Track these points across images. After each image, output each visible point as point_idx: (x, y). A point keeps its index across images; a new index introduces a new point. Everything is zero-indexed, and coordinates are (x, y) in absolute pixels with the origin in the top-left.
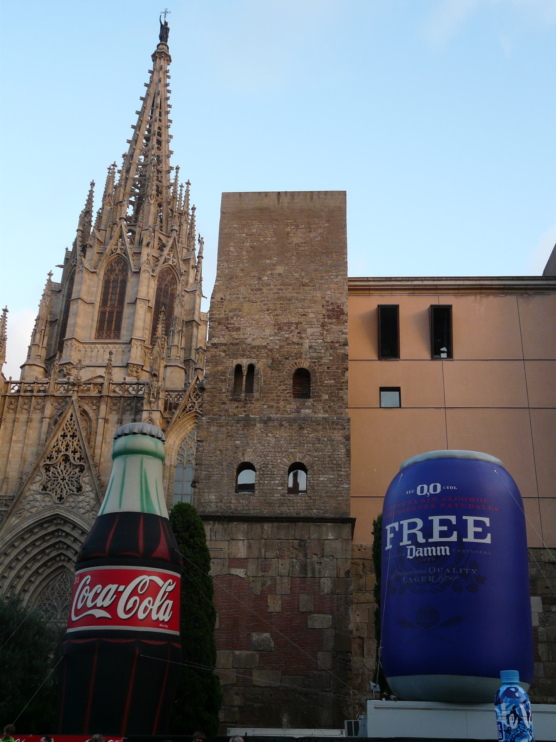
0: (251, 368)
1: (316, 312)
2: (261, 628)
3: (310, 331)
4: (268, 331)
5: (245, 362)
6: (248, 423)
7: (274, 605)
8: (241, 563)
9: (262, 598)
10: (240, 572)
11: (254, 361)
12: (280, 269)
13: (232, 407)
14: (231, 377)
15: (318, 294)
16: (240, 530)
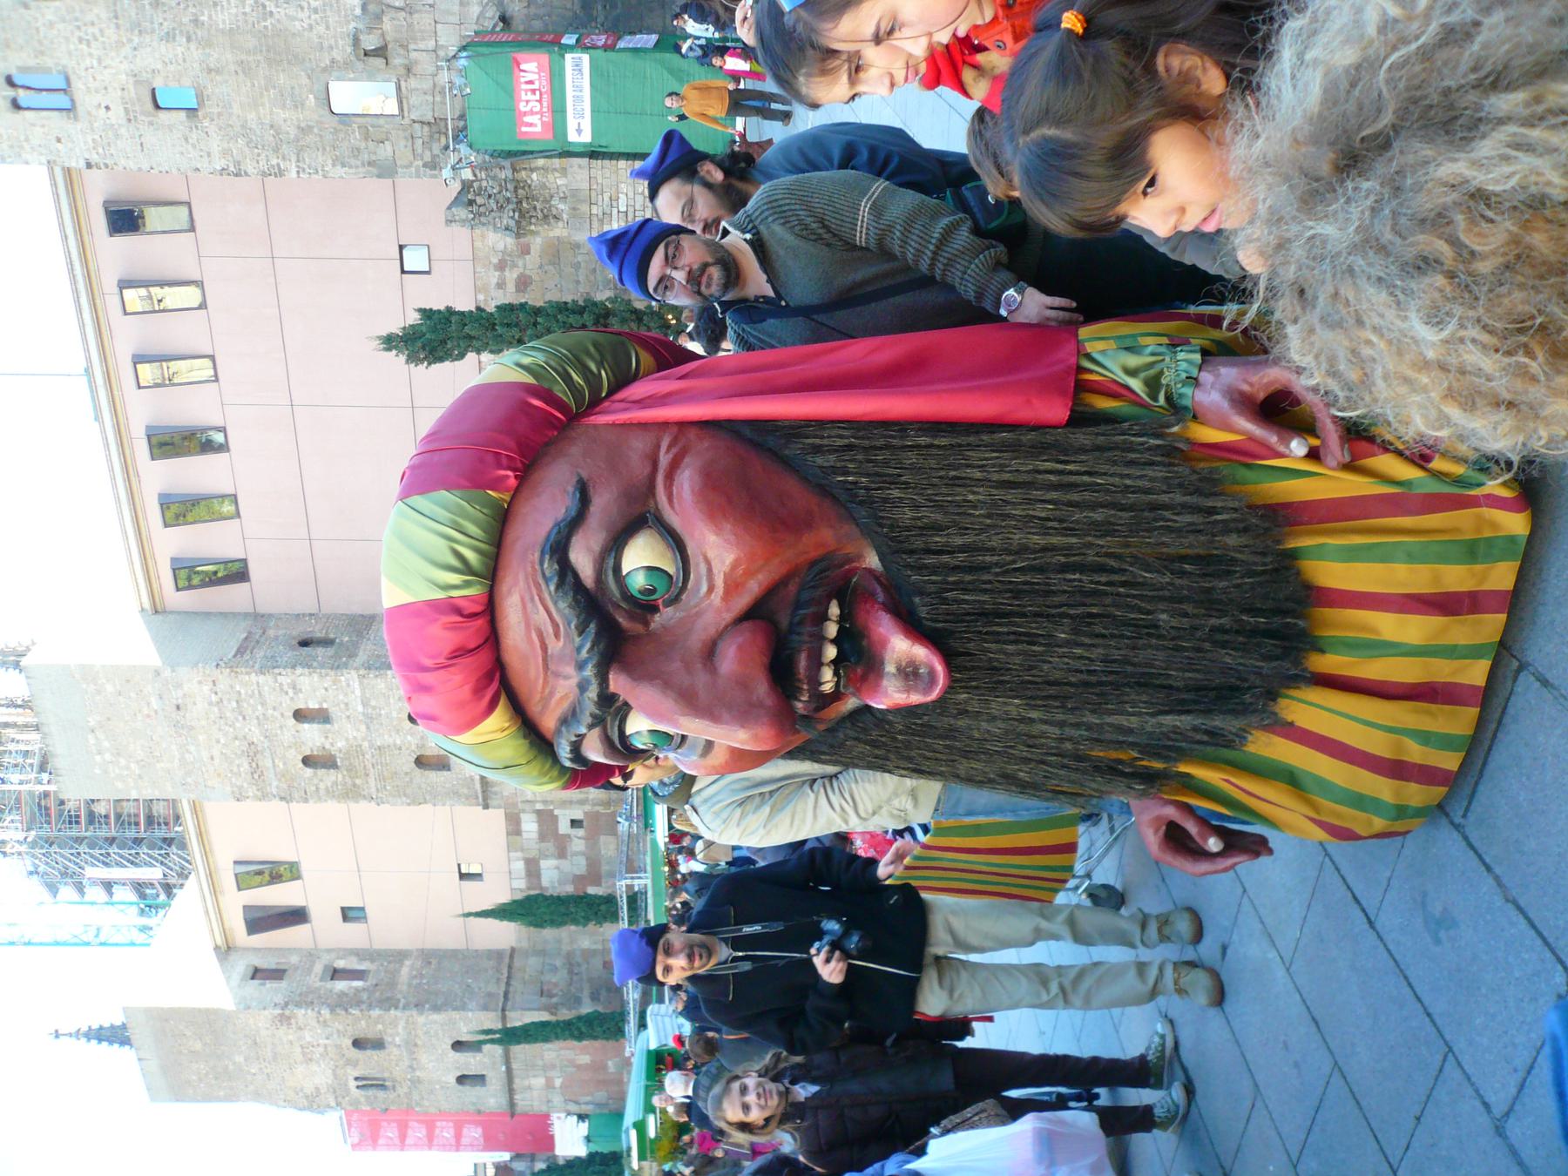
0: (356, 1079)
1: (286, 1034)
2: (604, 1067)
3: (308, 1039)
4: (314, 1067)
5: (353, 1084)
6: (416, 1082)
7: (585, 1059)
8: (549, 1085)
9: (579, 1067)
10: (558, 1082)
11: (351, 1078)
12: (239, 1059)
13: (402, 1091)
14: (371, 1092)
15: (264, 1033)
16: (517, 1083)
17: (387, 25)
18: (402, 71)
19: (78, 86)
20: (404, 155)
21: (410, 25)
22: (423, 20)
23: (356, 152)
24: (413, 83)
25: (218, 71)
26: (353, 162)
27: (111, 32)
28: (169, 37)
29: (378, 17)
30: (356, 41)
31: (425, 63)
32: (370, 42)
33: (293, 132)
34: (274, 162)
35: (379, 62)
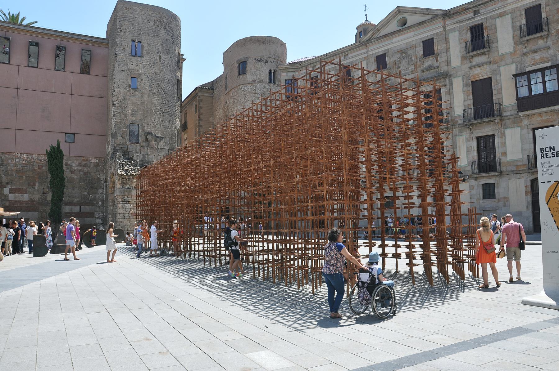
17: (154, 142)
18: (142, 144)
19: (139, 59)
20: (118, 142)
21: (154, 148)
22: (155, 153)
23: (119, 128)
24: (138, 147)
25: (142, 96)
26: (117, 127)
27: (151, 71)
28: (151, 86)
29: (156, 141)
30: (150, 133)
31: (144, 151)
32: (149, 137)
33: (125, 112)
34: (117, 105)
35: (144, 138)
